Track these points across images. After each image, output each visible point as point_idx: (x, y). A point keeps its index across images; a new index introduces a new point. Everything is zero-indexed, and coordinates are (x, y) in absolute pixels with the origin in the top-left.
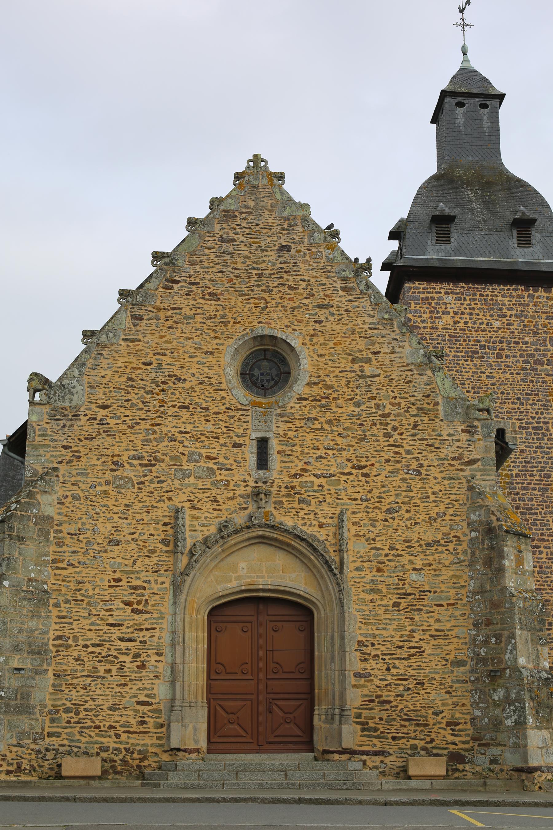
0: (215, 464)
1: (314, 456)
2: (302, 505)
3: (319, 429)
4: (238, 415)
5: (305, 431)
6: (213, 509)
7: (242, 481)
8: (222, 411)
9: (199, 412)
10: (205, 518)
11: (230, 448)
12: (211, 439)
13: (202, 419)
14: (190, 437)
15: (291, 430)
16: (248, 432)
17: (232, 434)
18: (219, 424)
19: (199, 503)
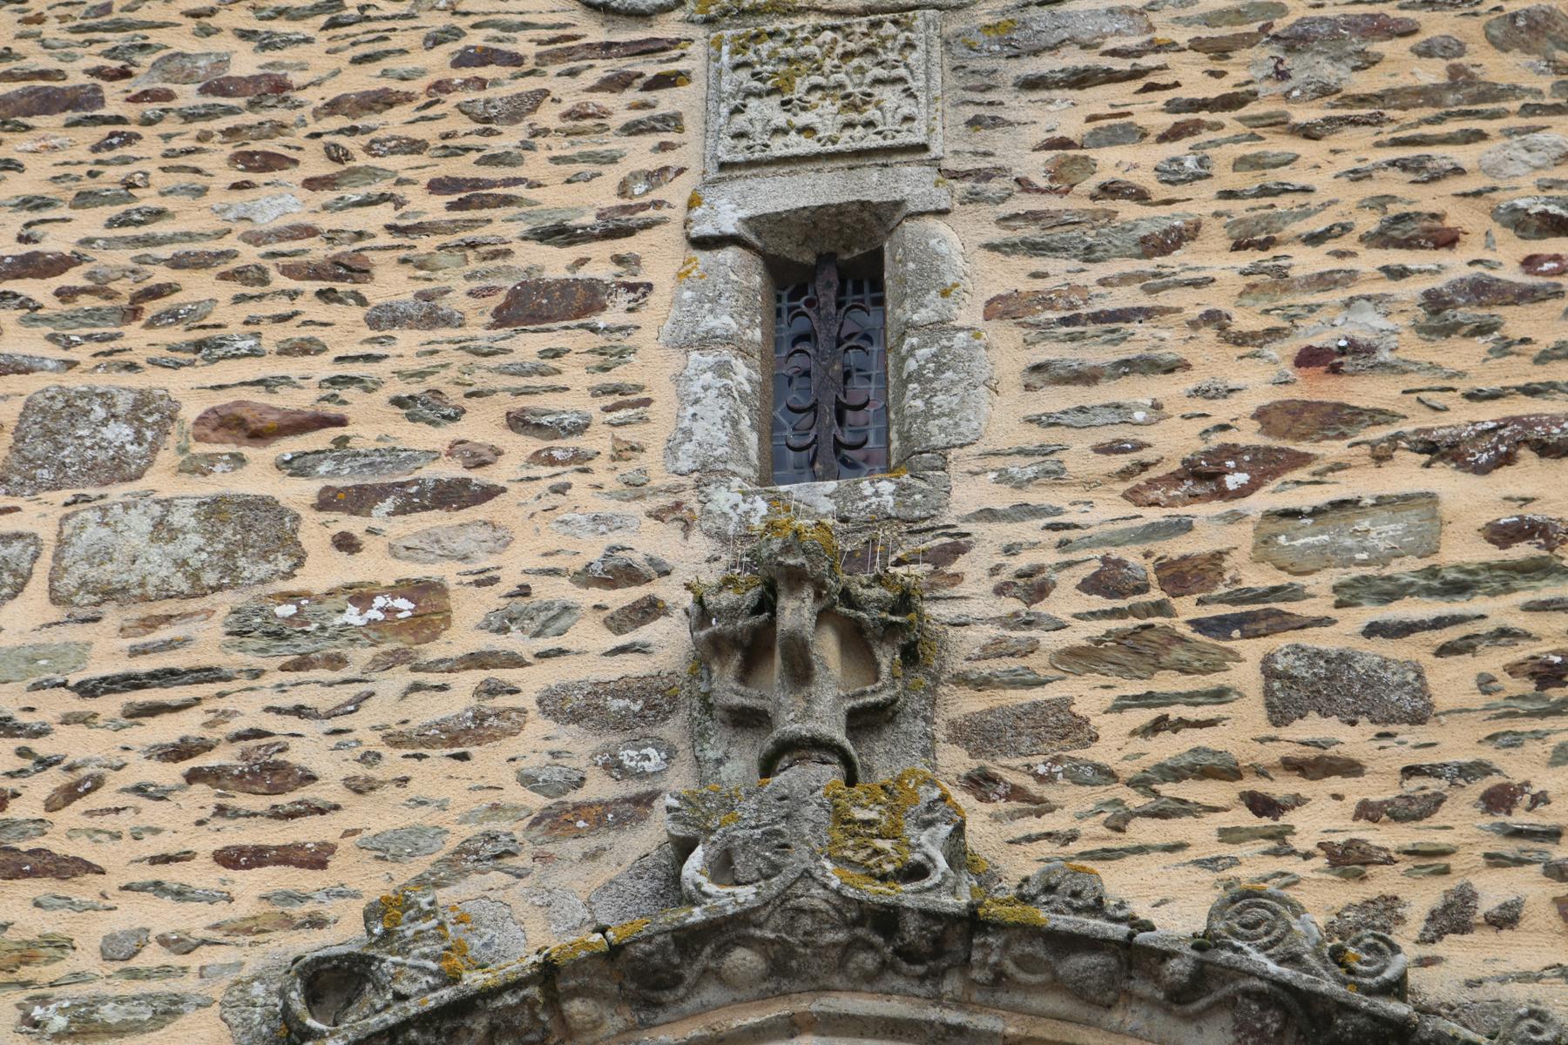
0: (297, 467)
1: (1410, 290)
2: (1312, 728)
3: (1427, 95)
4: (569, 93)
5: (1277, 123)
6: (229, 859)
7: (585, 578)
8: (417, 86)
9: (189, 117)
10: (120, 950)
11: (478, 330)
12: (280, 282)
13: (217, 161)
14: (64, 294)
15: (1124, 132)
16: (675, 193)
17: (501, 226)
18: (372, 174)
19: (72, 815)
